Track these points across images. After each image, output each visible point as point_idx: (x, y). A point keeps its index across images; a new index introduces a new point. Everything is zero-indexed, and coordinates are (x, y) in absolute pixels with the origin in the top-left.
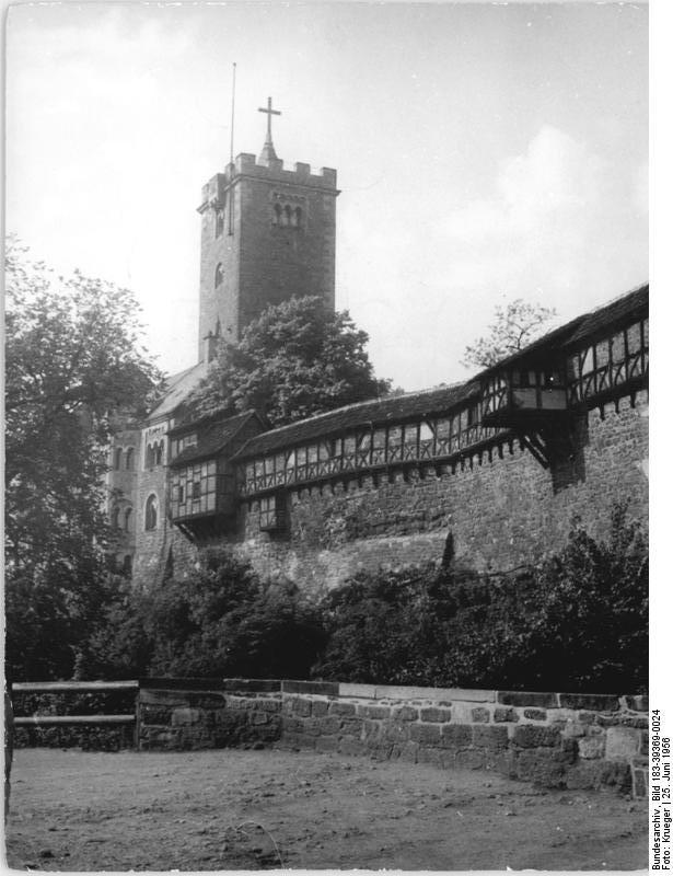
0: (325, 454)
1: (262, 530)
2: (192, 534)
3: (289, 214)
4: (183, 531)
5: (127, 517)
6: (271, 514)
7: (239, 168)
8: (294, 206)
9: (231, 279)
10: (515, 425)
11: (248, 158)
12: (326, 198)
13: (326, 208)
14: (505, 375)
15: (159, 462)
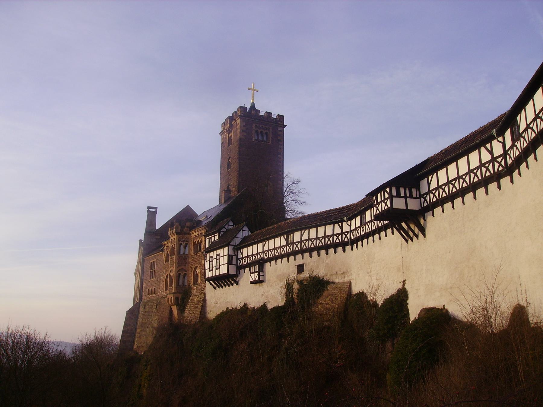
0: (284, 243)
1: (251, 283)
2: (215, 286)
3: (262, 136)
4: (211, 284)
5: (184, 278)
6: (256, 274)
7: (239, 113)
8: (264, 132)
9: (235, 165)
10: (394, 219)
11: (243, 109)
12: (280, 129)
13: (279, 133)
14: (388, 190)
15: (200, 250)
